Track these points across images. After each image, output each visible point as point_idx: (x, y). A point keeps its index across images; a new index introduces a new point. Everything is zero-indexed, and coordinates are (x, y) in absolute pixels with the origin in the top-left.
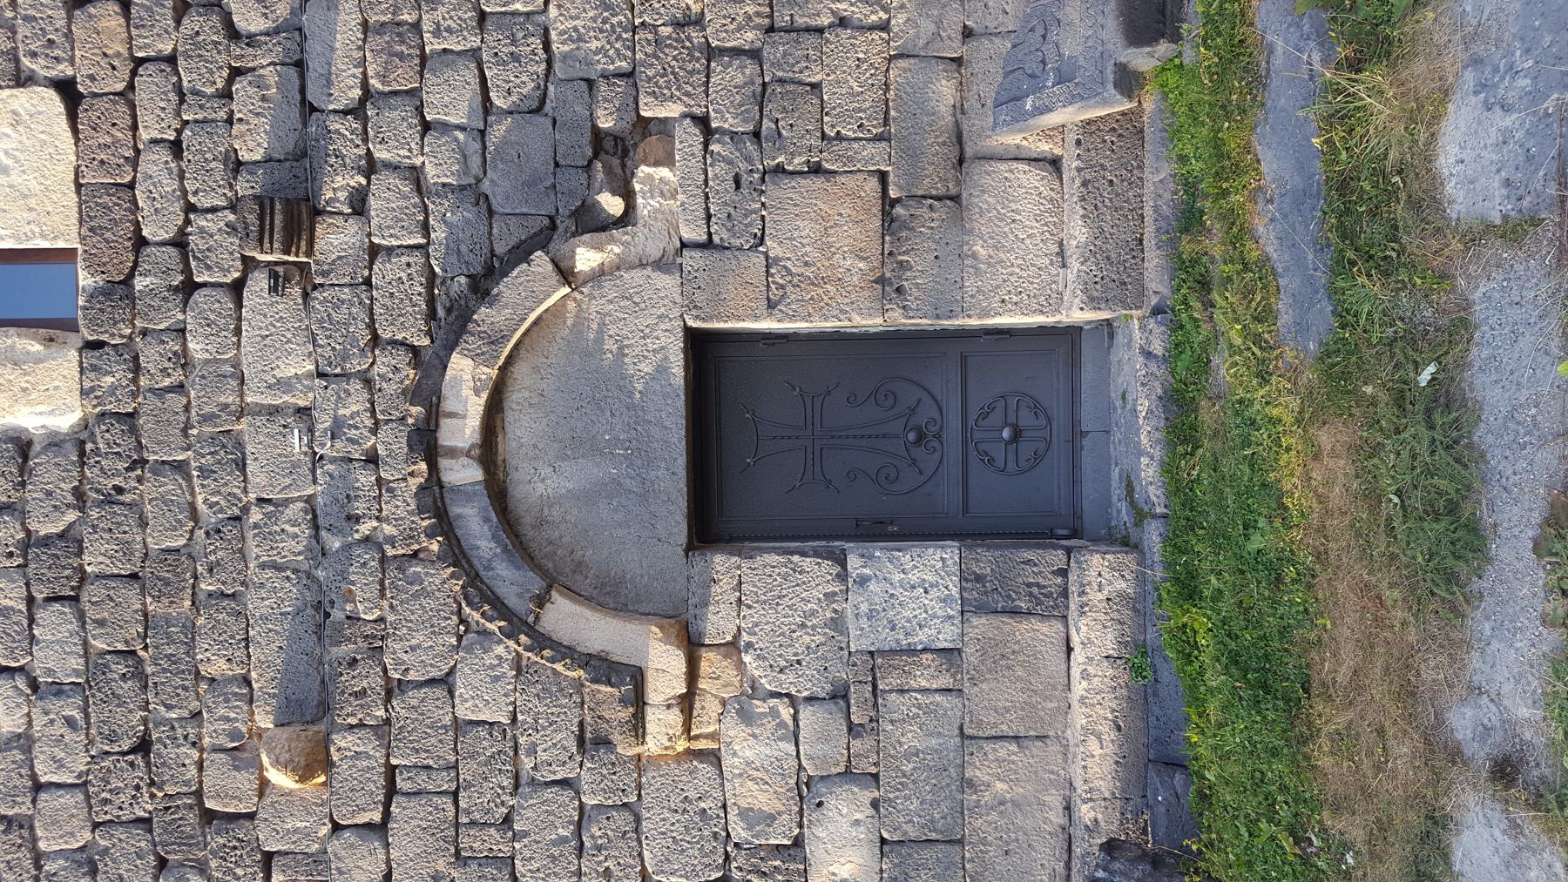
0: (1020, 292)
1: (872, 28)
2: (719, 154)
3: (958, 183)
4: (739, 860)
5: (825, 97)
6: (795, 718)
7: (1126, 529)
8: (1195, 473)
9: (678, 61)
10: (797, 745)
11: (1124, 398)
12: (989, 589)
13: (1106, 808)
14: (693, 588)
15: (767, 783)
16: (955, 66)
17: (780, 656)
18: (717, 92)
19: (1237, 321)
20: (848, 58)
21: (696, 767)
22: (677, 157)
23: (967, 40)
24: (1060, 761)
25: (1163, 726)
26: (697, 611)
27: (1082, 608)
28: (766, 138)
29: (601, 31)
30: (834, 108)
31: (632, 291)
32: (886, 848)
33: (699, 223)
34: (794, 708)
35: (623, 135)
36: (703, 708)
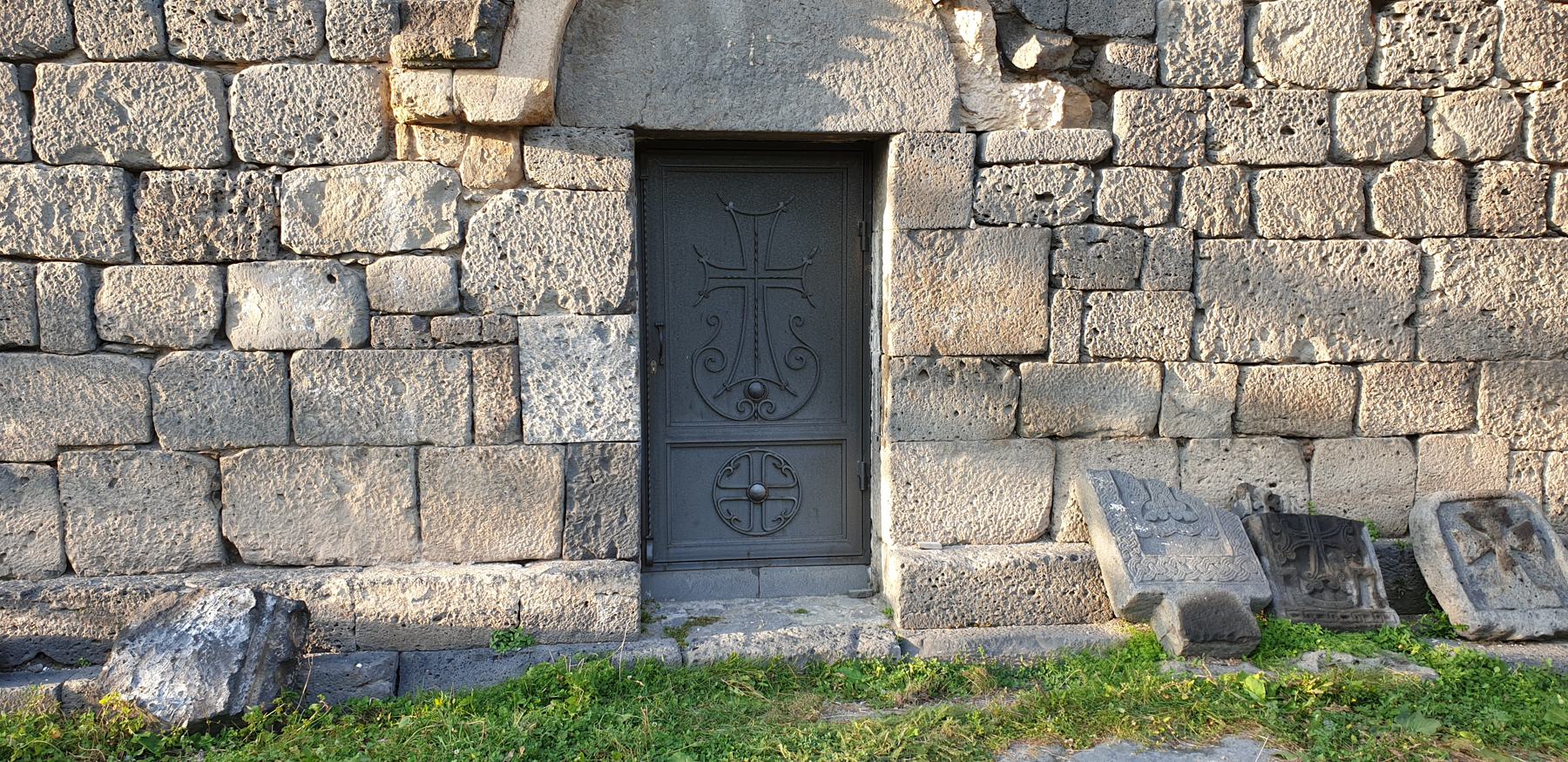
0: (917, 501)
1: (1192, 342)
2: (1075, 177)
3: (1032, 435)
4: (260, 181)
5: (1126, 293)
6: (436, 251)
7: (659, 619)
8: (736, 690)
9: (1171, 134)
10: (403, 252)
11: (801, 611)
12: (592, 473)
13: (342, 607)
14: (592, 134)
15: (356, 216)
16: (1150, 429)
17: (511, 235)
18: (1137, 176)
19: (923, 730)
20: (1164, 318)
21: (373, 130)
22: (1072, 130)
24: (392, 554)
25: (442, 666)
26: (563, 137)
27: (576, 576)
28: (1088, 229)
29: (1204, 52)
30: (1115, 303)
31: (932, 73)
32: (280, 356)
33: (1003, 153)
34: (447, 250)
35: (1093, 71)
36: (446, 141)
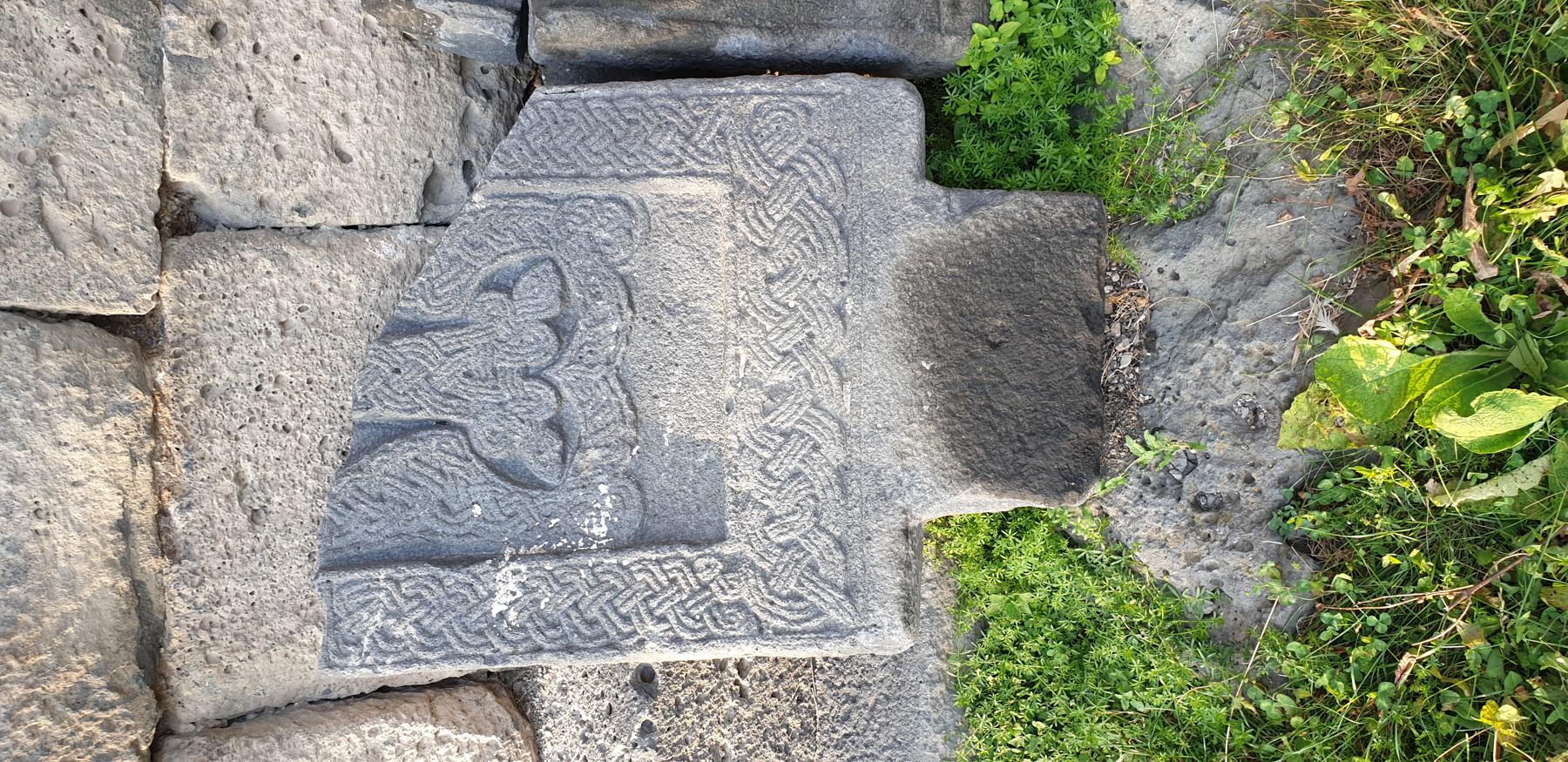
16: (121, 359)
23: (180, 244)
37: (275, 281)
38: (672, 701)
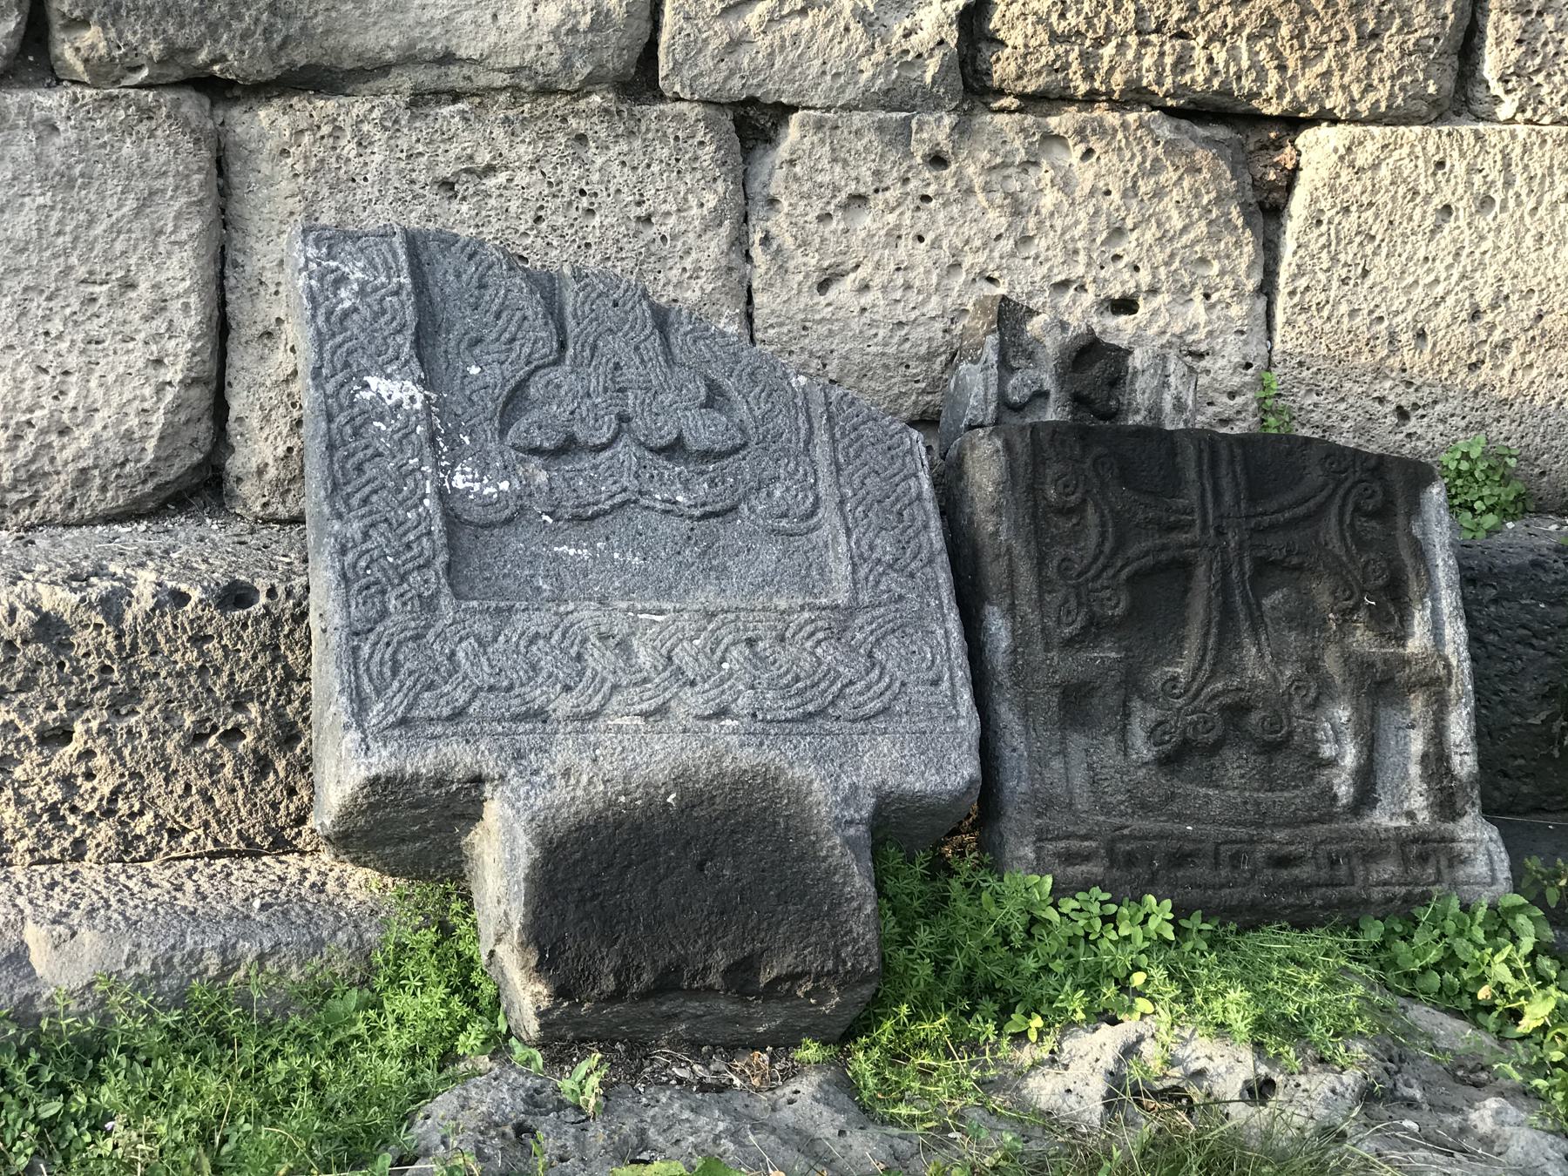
3: (103, 72)
16: (615, 59)
23: (727, 121)
37: (695, 211)
38: (210, 631)
